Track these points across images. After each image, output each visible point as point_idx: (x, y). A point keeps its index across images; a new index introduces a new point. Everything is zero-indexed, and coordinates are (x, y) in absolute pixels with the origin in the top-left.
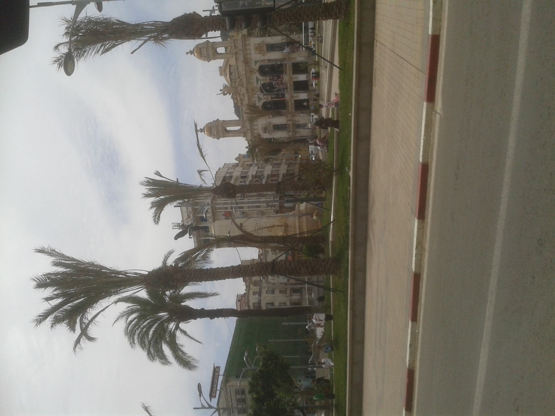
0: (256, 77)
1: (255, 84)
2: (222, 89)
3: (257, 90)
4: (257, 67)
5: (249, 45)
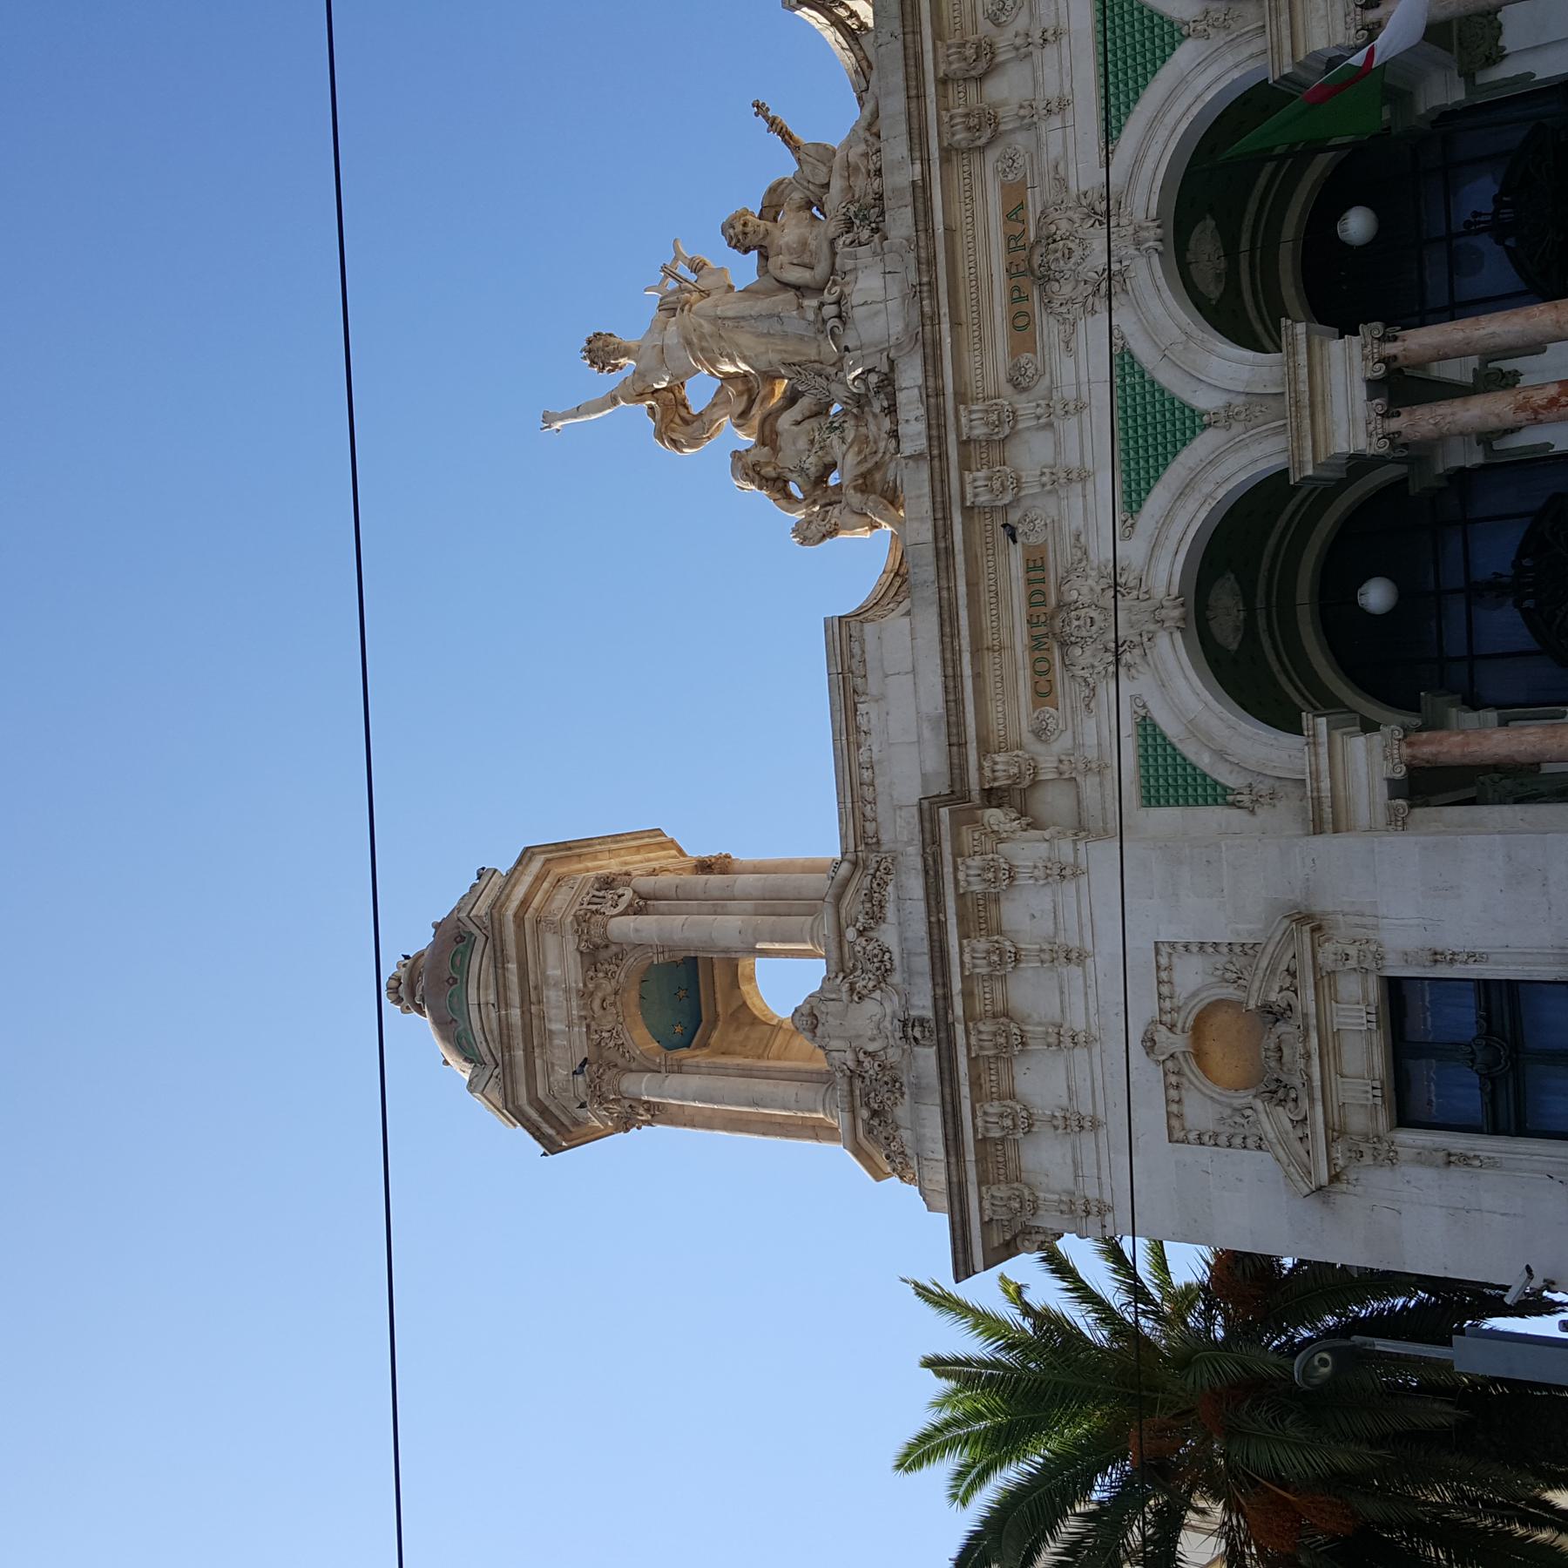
2: (633, 321)
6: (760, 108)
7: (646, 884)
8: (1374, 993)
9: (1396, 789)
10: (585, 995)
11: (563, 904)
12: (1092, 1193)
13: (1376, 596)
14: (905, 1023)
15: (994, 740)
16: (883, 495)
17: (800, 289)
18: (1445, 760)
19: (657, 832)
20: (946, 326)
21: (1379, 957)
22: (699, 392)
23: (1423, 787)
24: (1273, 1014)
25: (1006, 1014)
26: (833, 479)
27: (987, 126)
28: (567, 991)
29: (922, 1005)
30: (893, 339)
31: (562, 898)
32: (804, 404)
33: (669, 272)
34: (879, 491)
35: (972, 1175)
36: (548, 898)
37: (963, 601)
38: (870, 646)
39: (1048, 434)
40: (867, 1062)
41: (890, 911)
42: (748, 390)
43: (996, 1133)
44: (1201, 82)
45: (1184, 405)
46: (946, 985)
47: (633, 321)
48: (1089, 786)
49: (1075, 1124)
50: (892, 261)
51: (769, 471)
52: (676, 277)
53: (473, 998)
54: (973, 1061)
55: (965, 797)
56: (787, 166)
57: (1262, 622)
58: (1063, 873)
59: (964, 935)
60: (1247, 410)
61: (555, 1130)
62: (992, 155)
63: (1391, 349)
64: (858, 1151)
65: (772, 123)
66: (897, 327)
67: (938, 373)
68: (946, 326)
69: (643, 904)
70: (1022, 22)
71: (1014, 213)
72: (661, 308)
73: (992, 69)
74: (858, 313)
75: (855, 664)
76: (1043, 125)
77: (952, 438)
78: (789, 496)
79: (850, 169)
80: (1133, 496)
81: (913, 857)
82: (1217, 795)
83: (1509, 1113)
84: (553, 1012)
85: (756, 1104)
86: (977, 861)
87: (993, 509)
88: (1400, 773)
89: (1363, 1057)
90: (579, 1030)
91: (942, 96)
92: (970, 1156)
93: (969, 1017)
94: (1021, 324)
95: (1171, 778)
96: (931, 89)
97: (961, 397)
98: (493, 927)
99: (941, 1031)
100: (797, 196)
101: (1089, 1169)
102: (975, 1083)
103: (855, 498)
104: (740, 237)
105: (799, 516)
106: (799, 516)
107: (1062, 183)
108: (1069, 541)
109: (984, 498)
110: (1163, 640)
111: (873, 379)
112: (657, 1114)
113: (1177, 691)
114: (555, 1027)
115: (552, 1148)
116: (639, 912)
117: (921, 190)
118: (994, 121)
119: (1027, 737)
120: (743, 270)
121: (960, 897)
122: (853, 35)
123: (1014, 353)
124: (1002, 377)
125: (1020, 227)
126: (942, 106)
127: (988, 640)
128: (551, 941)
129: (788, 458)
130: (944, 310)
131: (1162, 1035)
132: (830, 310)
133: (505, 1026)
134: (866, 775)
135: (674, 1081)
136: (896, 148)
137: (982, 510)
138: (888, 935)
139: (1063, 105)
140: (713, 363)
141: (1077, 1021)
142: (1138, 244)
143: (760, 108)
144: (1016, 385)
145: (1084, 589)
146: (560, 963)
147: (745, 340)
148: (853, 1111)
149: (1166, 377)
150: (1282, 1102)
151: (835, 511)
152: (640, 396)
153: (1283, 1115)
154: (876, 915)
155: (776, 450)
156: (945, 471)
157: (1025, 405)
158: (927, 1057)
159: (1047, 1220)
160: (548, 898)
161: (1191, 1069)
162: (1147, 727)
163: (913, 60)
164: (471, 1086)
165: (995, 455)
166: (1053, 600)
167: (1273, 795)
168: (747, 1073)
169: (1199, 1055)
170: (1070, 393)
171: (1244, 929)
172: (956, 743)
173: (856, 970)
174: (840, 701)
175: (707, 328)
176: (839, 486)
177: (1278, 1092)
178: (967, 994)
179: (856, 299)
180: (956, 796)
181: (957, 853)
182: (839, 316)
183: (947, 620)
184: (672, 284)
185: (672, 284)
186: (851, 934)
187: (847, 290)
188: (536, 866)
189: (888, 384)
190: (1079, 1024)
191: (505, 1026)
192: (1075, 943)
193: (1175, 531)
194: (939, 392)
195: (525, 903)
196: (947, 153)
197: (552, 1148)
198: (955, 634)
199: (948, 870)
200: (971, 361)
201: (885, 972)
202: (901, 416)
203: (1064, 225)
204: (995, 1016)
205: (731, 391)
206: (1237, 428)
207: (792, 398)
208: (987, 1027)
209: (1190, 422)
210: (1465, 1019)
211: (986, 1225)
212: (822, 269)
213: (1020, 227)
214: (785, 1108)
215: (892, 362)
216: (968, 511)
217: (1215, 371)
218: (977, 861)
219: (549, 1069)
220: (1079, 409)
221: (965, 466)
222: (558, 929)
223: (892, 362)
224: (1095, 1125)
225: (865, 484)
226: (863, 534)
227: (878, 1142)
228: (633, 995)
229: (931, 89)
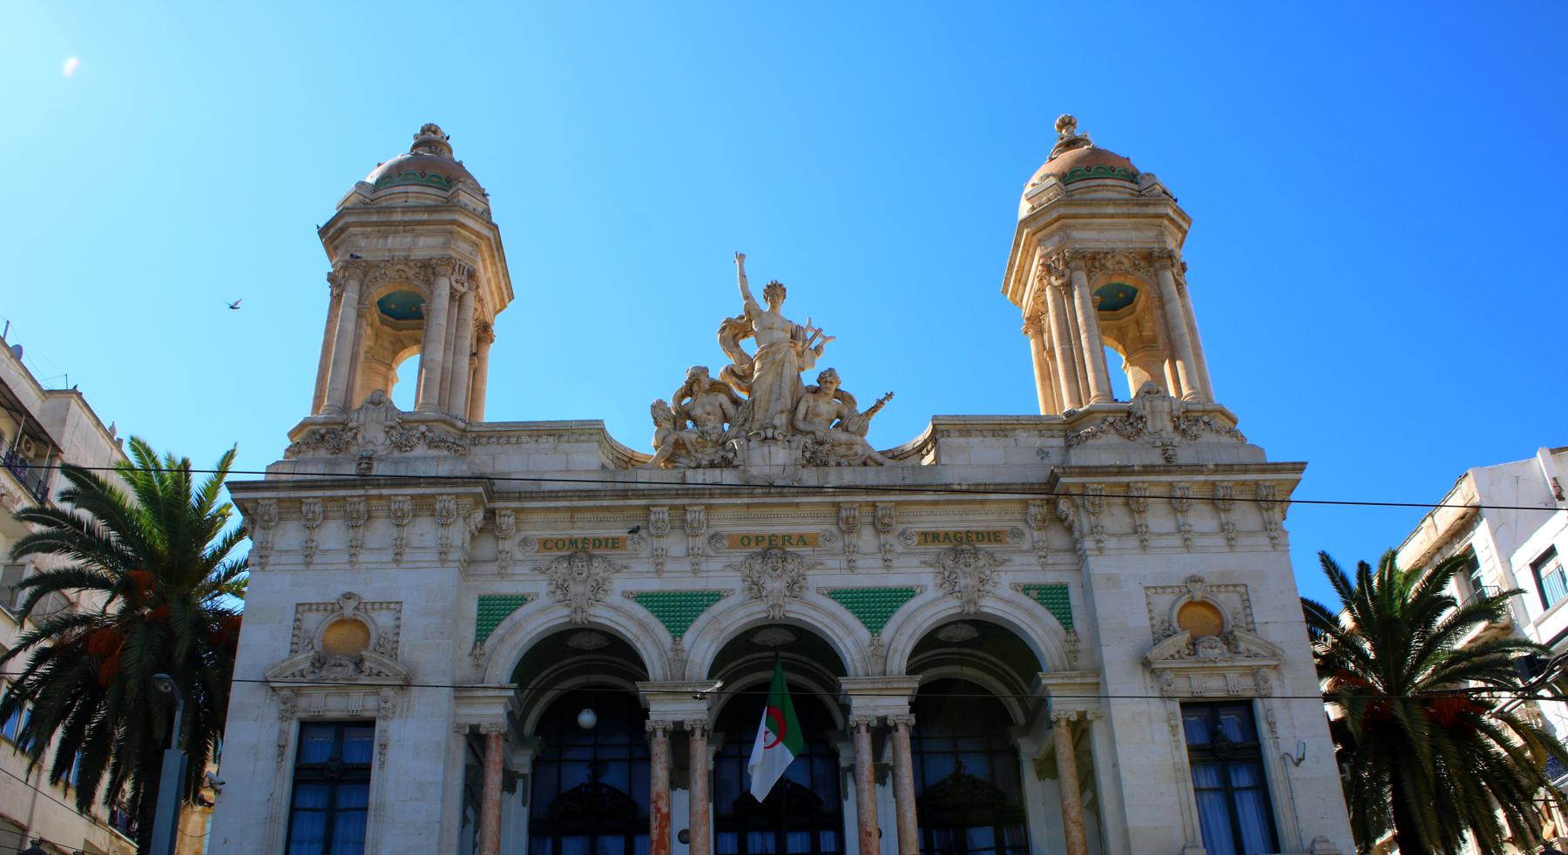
0: (907, 594)
1: (829, 573)
2: (792, 311)
3: (775, 585)
4: (1004, 598)
5: (1229, 533)
6: (889, 396)
7: (470, 302)
8: (368, 714)
10: (406, 260)
11: (460, 250)
12: (272, 560)
13: (587, 718)
14: (370, 458)
15: (523, 516)
16: (673, 454)
17: (795, 409)
18: (488, 753)
19: (511, 297)
20: (746, 500)
21: (385, 718)
22: (749, 346)
23: (476, 740)
24: (359, 663)
25: (370, 517)
26: (689, 424)
27: (848, 527)
28: (409, 249)
29: (379, 469)
31: (465, 248)
32: (730, 409)
33: (818, 332)
34: (674, 451)
35: (282, 495)
36: (466, 239)
37: (598, 503)
38: (585, 446)
39: (683, 553)
40: (351, 434)
41: (434, 452)
42: (743, 377)
43: (304, 509)
44: (848, 641)
45: (687, 627)
46: (386, 486)
47: (792, 311)
48: (493, 568)
49: (309, 553)
50: (790, 470)
51: (695, 388)
52: (813, 338)
54: (344, 498)
55: (490, 499)
56: (862, 408)
57: (586, 657)
58: (443, 554)
59: (413, 497)
60: (678, 659)
61: (332, 234)
62: (834, 529)
64: (302, 426)
65: (880, 403)
66: (755, 471)
67: (722, 495)
68: (746, 500)
69: (457, 298)
70: (899, 548)
71: (802, 540)
72: (798, 327)
73: (878, 532)
74: (766, 449)
76: (843, 558)
77: (687, 501)
78: (683, 397)
79: (851, 445)
80: (643, 599)
81: (462, 469)
82: (482, 636)
83: (304, 775)
84: (398, 240)
85: (335, 363)
86: (452, 506)
87: (648, 521)
88: (483, 731)
89: (336, 706)
90: (386, 255)
91: (867, 504)
92: (293, 494)
93: (369, 497)
94: (745, 541)
95: (493, 611)
96: (870, 498)
97: (708, 507)
98: (450, 205)
99: (365, 479)
100: (845, 411)
101: (284, 559)
102: (332, 499)
103: (671, 439)
104: (827, 377)
105: (670, 403)
106: (670, 403)
107: (812, 567)
108: (625, 562)
109: (653, 517)
110: (566, 611)
111: (730, 455)
112: (336, 299)
113: (537, 619)
114: (390, 240)
115: (323, 232)
116: (452, 296)
117: (819, 490)
118: (850, 531)
119: (523, 534)
120: (810, 378)
121: (433, 496)
122: (920, 451)
123: (730, 536)
126: (861, 504)
127: (578, 516)
128: (439, 240)
129: (703, 398)
130: (755, 500)
131: (353, 603)
132: (770, 434)
133: (390, 210)
135: (353, 314)
136: (849, 477)
137: (648, 516)
138: (421, 450)
139: (852, 569)
140: (760, 358)
141: (364, 557)
142: (773, 606)
143: (889, 396)
144: (712, 537)
145: (598, 568)
146: (426, 246)
147: (770, 378)
148: (325, 424)
149: (704, 618)
150: (313, 665)
151: (669, 425)
152: (748, 313)
153: (306, 665)
154: (432, 444)
155: (707, 392)
156: (670, 497)
157: (700, 542)
158: (350, 469)
159: (258, 533)
160: (466, 239)
161: (335, 617)
162: (521, 600)
164: (361, 185)
165: (677, 523)
167: (478, 666)
168: (354, 359)
169: (342, 622)
170: (704, 566)
171: (405, 651)
172: (521, 496)
173: (403, 429)
175: (779, 357)
176: (685, 427)
177: (319, 663)
178: (381, 497)
179: (773, 448)
180: (492, 495)
181: (458, 495)
183: (591, 494)
184: (810, 334)
185: (810, 334)
186: (423, 428)
188: (486, 232)
189: (727, 463)
190: (361, 558)
191: (390, 210)
192: (406, 558)
193: (623, 620)
194: (712, 496)
195: (463, 226)
196: (837, 505)
197: (323, 232)
198: (580, 498)
199: (449, 490)
200: (728, 513)
201: (399, 446)
203: (791, 567)
204: (369, 511)
205: (746, 366)
206: (671, 654)
207: (736, 402)
208: (362, 507)
209: (677, 631)
210: (353, 757)
211: (255, 500)
212: (801, 425)
215: (737, 467)
216: (647, 507)
217: (702, 645)
218: (452, 506)
219: (366, 236)
220: (694, 572)
221: (671, 507)
222: (446, 246)
223: (737, 467)
224: (308, 564)
225: (679, 444)
226: (653, 441)
227: (308, 437)
228: (405, 288)
229: (870, 498)
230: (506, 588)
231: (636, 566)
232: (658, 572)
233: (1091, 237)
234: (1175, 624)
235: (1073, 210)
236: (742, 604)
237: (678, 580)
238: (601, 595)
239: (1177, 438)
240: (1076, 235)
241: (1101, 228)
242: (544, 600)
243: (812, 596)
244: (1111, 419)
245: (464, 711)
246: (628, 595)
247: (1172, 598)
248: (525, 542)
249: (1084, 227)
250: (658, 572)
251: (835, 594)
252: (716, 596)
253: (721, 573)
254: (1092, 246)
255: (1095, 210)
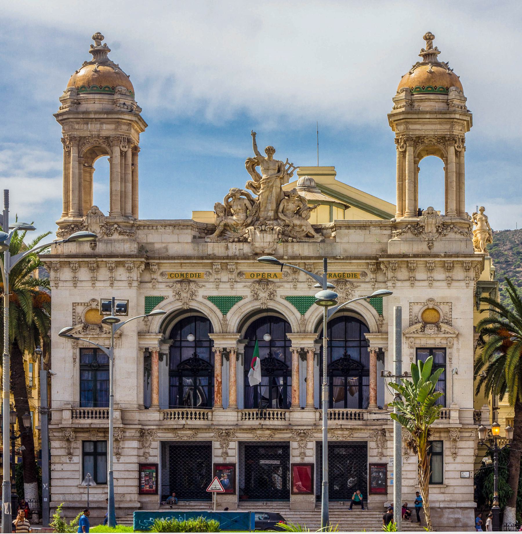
3: (263, 295)
9: (147, 349)
10: (98, 136)
30: (254, 243)
31: (124, 127)
45: (228, 310)
48: (150, 285)
53: (97, 96)
60: (224, 323)
63: (232, 352)
68: (252, 261)
75: (181, 227)
80: (211, 299)
88: (150, 350)
94: (252, 275)
95: (151, 302)
107: (279, 287)
108: (203, 284)
110: (180, 304)
112: (68, 154)
113: (169, 306)
124: (242, 270)
125: (272, 276)
128: (113, 126)
134: (155, 228)
142: (262, 303)
145: (192, 286)
149: (235, 307)
163: (309, 258)
166: (191, 279)
174: (173, 222)
179: (265, 235)
182: (262, 230)
187: (268, 232)
202: (237, 244)
206: (222, 322)
209: (225, 313)
213: (272, 276)
214: (72, 199)
217: (234, 317)
219: (78, 123)
220: (232, 288)
229: (303, 261)
230: (155, 293)
231: (208, 285)
232: (217, 288)
233: (418, 129)
234: (420, 317)
235: (409, 116)
236: (250, 302)
237: (225, 291)
238: (194, 297)
239: (437, 235)
240: (411, 127)
241: (424, 124)
242: (171, 299)
243: (278, 299)
244: (409, 226)
245: (142, 342)
246: (204, 297)
247: (421, 306)
248: (162, 274)
249: (415, 123)
250: (217, 288)
251: (288, 298)
252: (240, 298)
253: (241, 289)
254: (418, 133)
255: (420, 116)
